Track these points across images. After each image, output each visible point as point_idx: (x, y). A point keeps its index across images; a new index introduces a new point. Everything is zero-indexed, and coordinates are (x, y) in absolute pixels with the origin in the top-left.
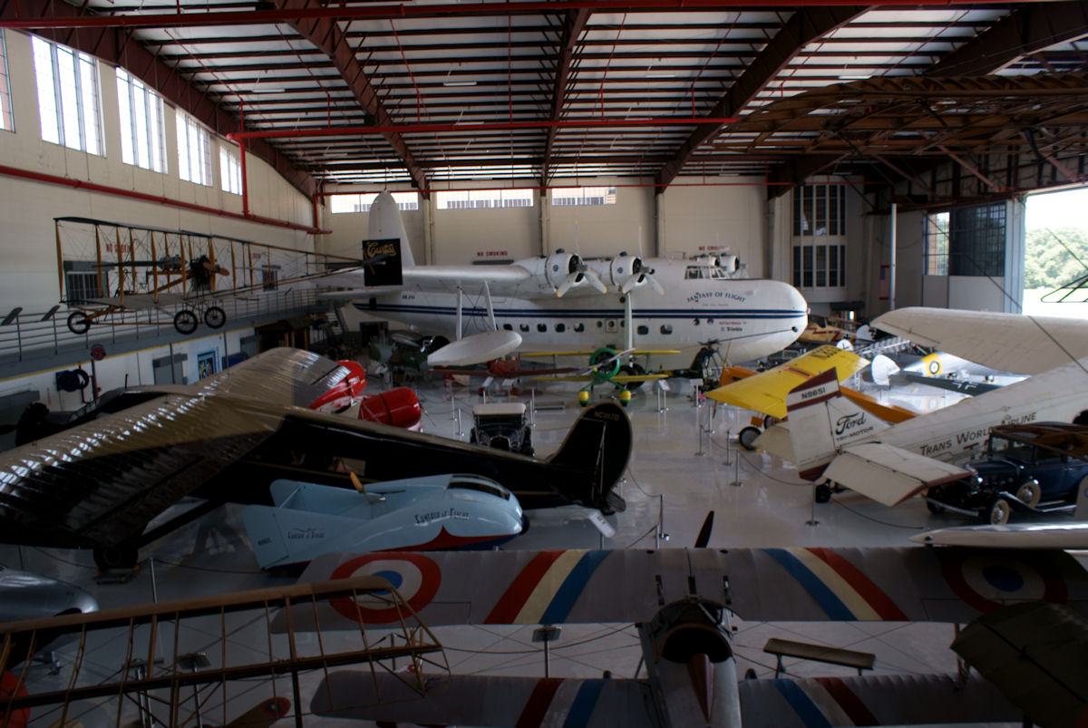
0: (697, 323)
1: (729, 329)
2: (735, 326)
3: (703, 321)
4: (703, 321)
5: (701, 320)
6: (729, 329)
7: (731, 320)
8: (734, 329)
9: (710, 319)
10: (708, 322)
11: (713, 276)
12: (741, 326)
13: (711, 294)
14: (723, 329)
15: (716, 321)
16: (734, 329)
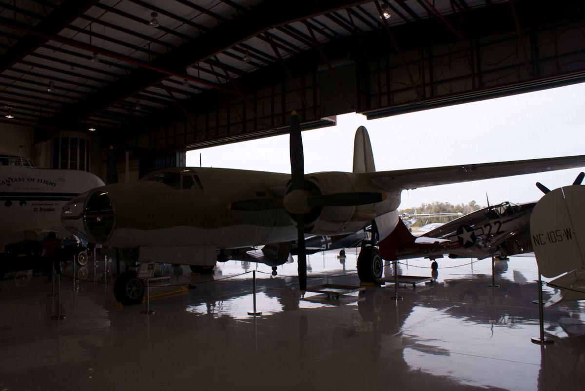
0: (8, 204)
1: (41, 209)
2: (47, 207)
3: (16, 203)
4: (16, 203)
5: (13, 202)
6: (41, 209)
7: (44, 202)
8: (47, 210)
9: (23, 201)
10: (21, 204)
11: (25, 165)
12: (54, 207)
13: (23, 179)
14: (36, 210)
15: (29, 203)
16: (47, 210)
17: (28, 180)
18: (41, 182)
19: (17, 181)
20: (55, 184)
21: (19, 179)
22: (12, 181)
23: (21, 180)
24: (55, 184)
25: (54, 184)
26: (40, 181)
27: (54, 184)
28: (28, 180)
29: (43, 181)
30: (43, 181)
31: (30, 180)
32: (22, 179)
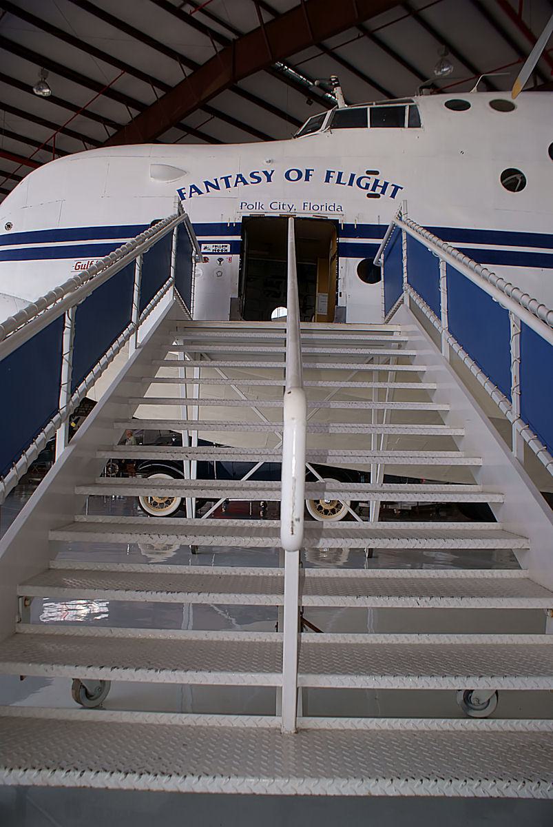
17: (287, 176)
18: (339, 182)
19: (245, 183)
20: (397, 188)
21: (252, 175)
22: (228, 186)
23: (259, 180)
24: (397, 188)
25: (390, 190)
26: (335, 176)
27: (390, 190)
28: (287, 176)
29: (345, 179)
30: (345, 179)
31: (293, 175)
32: (266, 173)
